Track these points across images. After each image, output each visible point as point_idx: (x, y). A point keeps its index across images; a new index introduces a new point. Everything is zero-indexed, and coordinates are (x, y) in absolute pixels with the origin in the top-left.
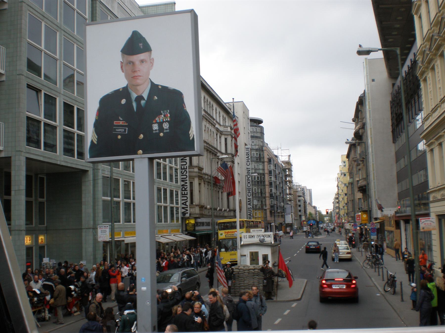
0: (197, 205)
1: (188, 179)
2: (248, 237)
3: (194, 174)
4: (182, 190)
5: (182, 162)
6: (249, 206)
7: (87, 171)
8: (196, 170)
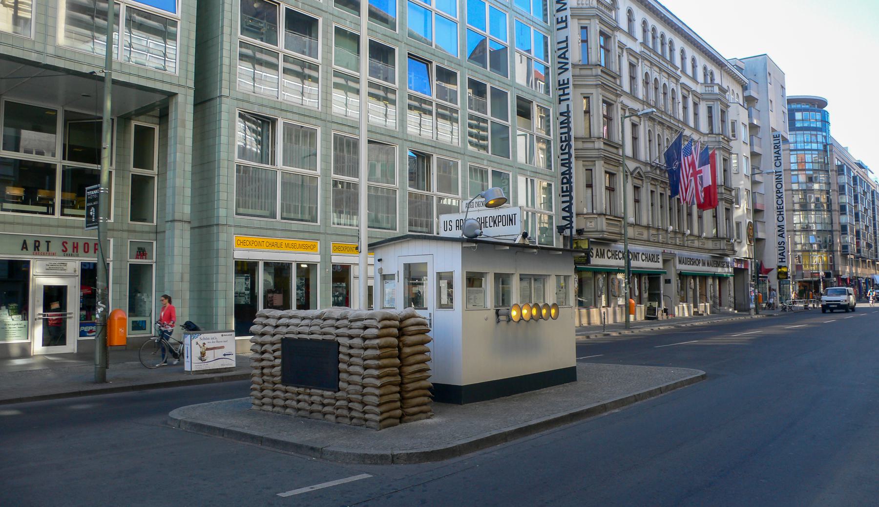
0: (600, 214)
1: (573, 159)
2: (454, 224)
3: (594, 153)
4: (563, 183)
5: (561, 128)
6: (781, 239)
7: (173, 95)
8: (600, 145)
